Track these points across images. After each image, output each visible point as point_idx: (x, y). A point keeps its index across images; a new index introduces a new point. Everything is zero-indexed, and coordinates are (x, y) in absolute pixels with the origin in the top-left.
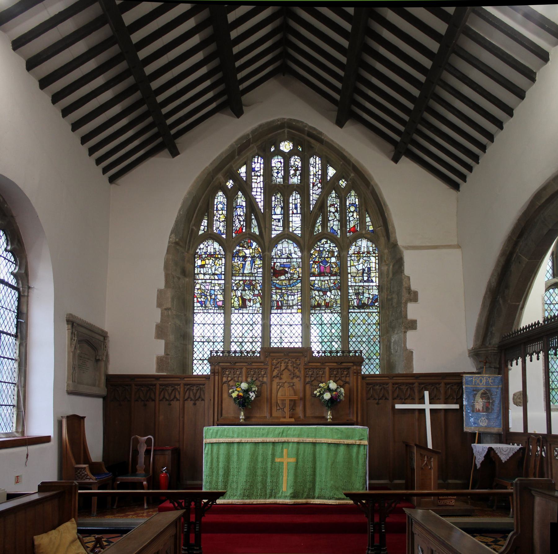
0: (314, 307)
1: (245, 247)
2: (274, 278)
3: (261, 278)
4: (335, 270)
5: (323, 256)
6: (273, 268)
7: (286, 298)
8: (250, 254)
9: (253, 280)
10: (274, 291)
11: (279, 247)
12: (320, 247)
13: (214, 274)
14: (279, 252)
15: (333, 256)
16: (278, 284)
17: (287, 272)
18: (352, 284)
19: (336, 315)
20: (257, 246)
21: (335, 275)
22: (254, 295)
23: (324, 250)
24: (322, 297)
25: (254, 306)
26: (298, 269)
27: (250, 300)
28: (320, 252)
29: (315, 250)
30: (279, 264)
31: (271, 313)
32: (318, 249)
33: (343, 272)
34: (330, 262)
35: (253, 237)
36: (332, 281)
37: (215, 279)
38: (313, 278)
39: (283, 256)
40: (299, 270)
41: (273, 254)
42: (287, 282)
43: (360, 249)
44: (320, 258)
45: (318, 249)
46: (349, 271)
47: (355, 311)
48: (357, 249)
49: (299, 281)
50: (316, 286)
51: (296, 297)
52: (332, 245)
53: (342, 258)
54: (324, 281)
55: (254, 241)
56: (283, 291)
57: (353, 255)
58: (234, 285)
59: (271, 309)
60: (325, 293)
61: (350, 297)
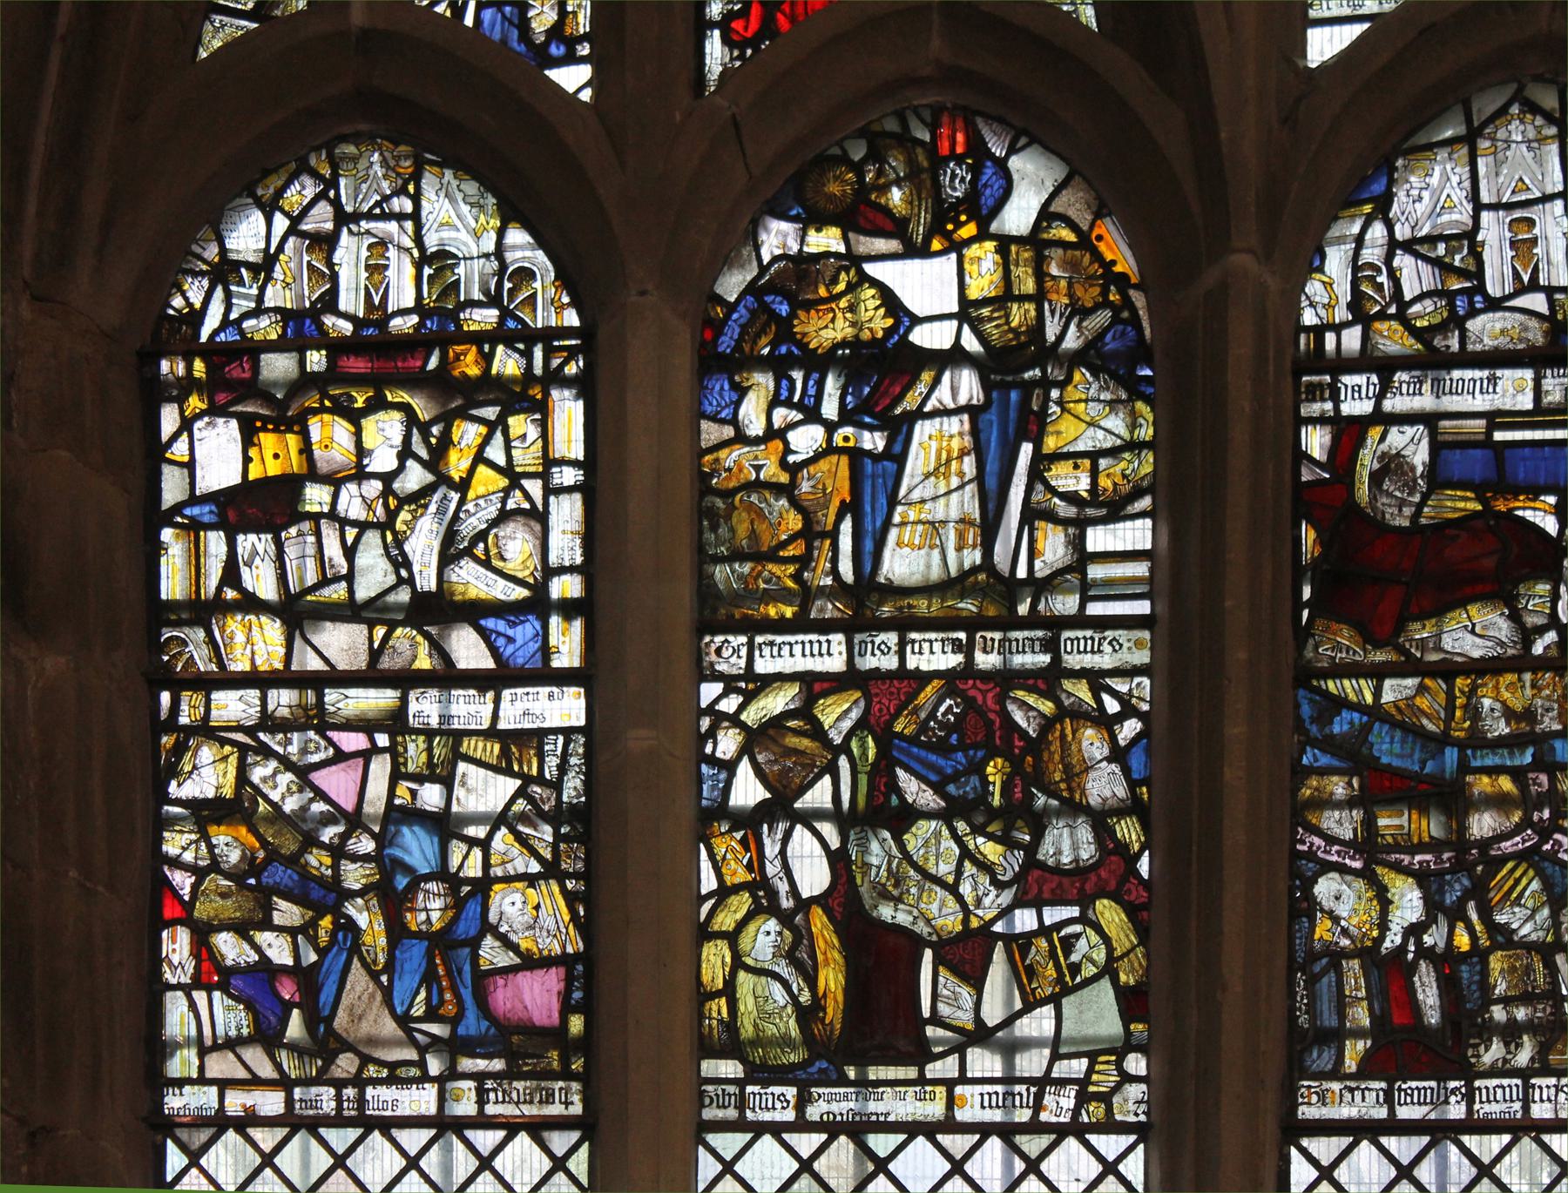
2: (1341, 643)
3: (1133, 650)
6: (1329, 502)
9: (1007, 679)
10: (1341, 823)
13: (436, 610)
16: (1401, 721)
22: (1037, 882)
25: (1040, 1023)
27: (967, 954)
30: (1413, 445)
37: (448, 677)
41: (1327, 290)
56: (1482, 824)
58: (727, 743)
59: (1295, 1070)
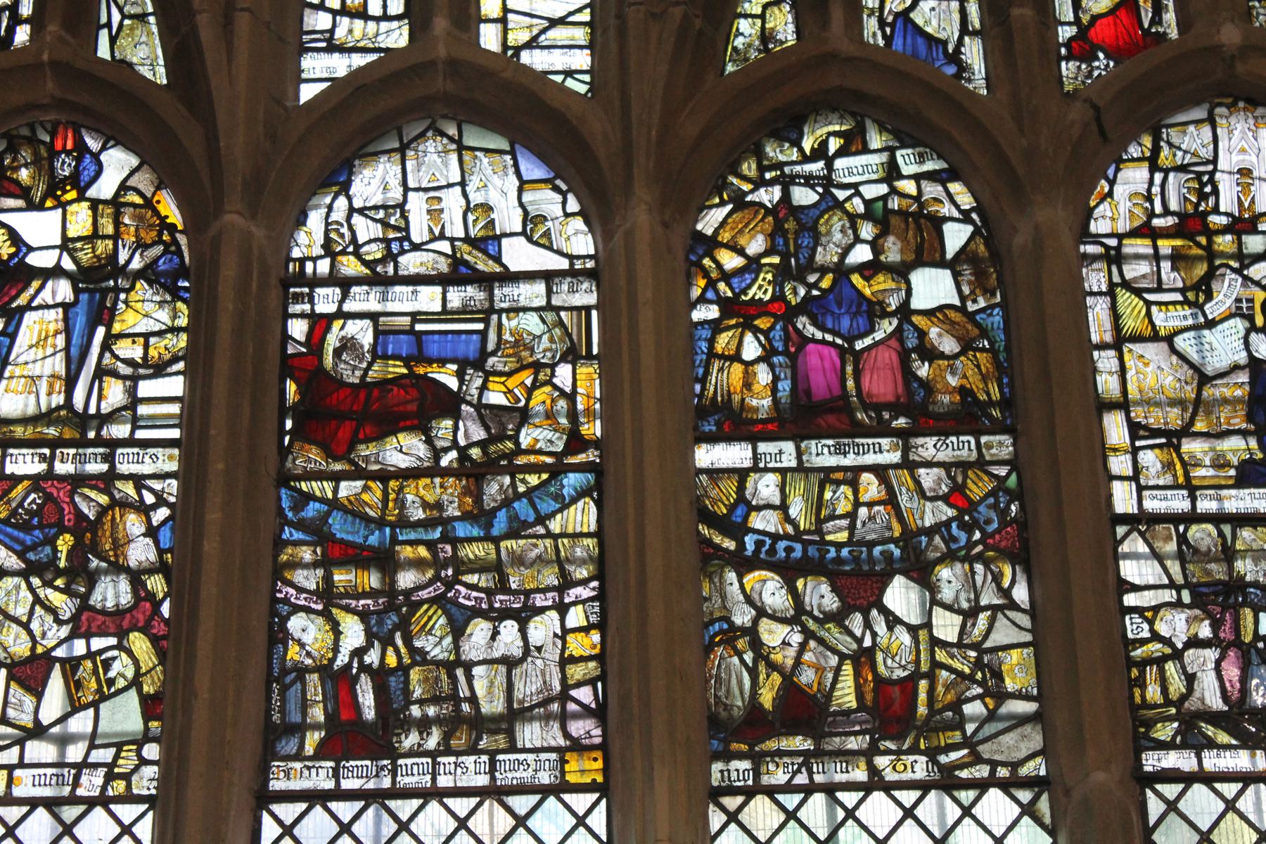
0: (752, 729)
1: (23, 192)
2: (312, 457)
3: (168, 461)
4: (955, 374)
5: (826, 255)
6: (308, 366)
7: (435, 645)
8: (66, 244)
9: (78, 481)
10: (309, 579)
11: (373, 182)
12: (786, 182)
14: (365, 229)
15: (928, 252)
16: (353, 510)
17: (449, 404)
18: (1153, 504)
19: (997, 807)
20: (144, 181)
21: (967, 416)
22: (85, 621)
23: (829, 204)
24: (833, 634)
25: (81, 723)
26: (563, 374)
28: (793, 230)
29: (740, 202)
30: (363, 333)
31: (265, 798)
32: (769, 196)
33: (1034, 381)
34: (905, 311)
35: (115, 105)
36: (928, 477)
38: (733, 455)
39: (411, 263)
40: (584, 381)
41: (309, 239)
42: (451, 497)
43: (1205, 185)
44: (783, 274)
45: (769, 196)
46: (1107, 384)
47: (1212, 761)
48: (1176, 191)
49: (572, 481)
50: (764, 522)
51: (542, 629)
52: (908, 162)
53: (1029, 285)
54: (852, 476)
55: (113, 138)
56: (406, 579)
57: (1141, 246)
59: (268, 755)
60: (860, 586)
61: (1135, 628)
